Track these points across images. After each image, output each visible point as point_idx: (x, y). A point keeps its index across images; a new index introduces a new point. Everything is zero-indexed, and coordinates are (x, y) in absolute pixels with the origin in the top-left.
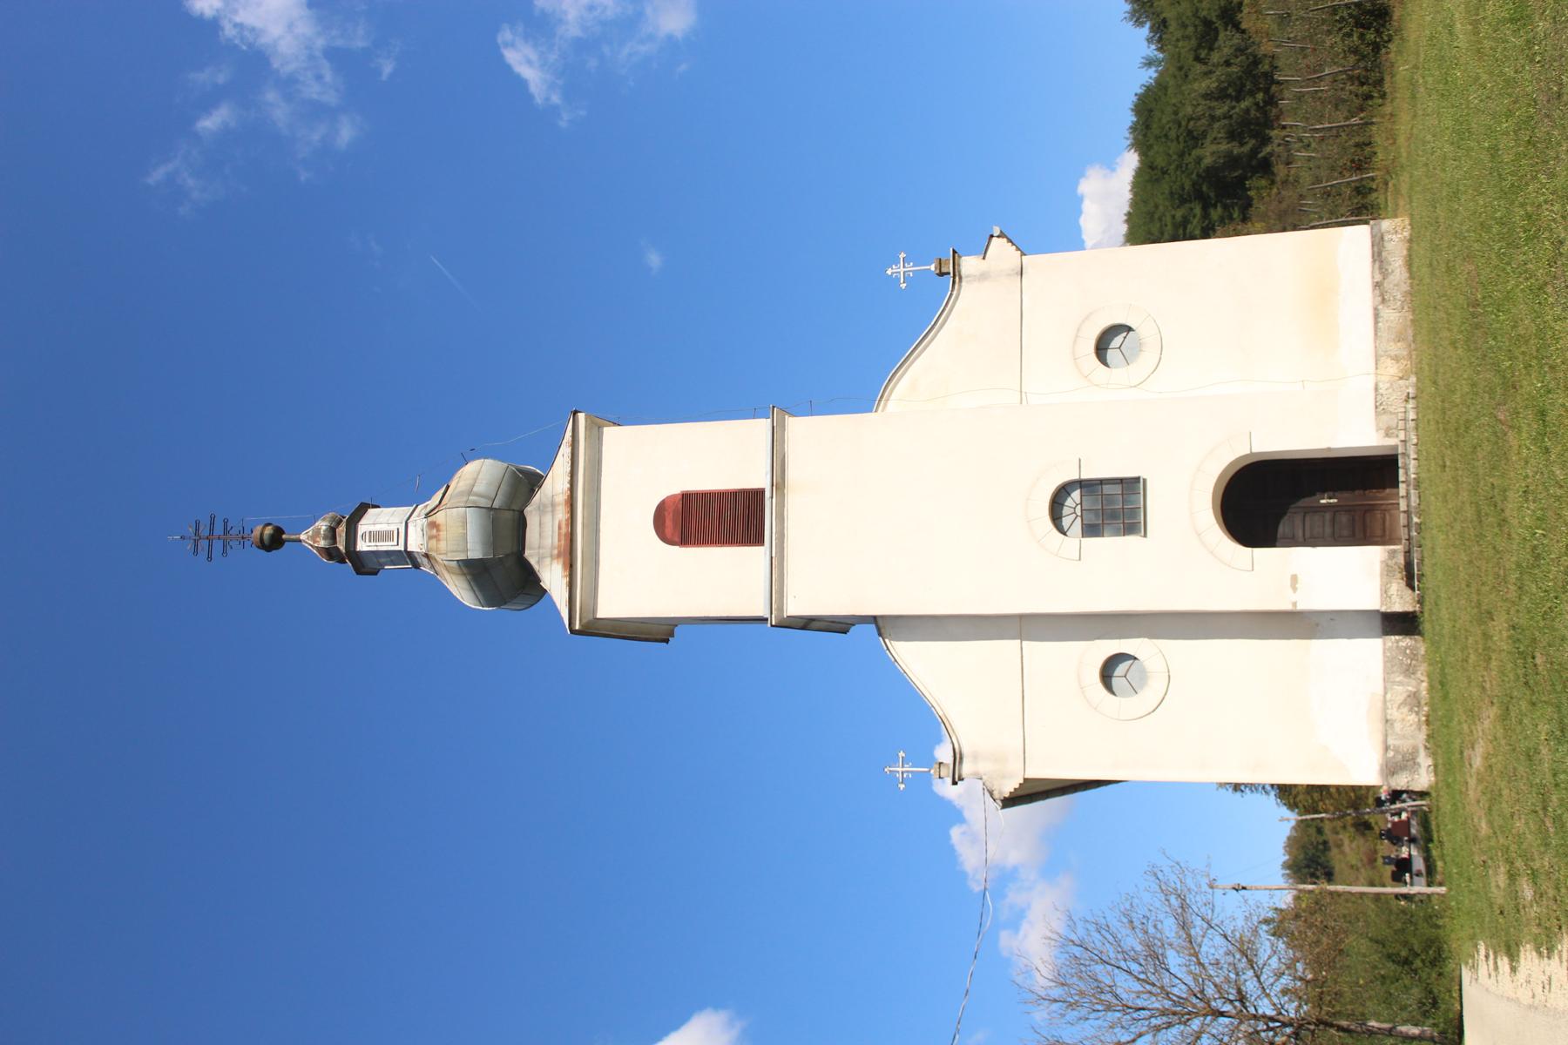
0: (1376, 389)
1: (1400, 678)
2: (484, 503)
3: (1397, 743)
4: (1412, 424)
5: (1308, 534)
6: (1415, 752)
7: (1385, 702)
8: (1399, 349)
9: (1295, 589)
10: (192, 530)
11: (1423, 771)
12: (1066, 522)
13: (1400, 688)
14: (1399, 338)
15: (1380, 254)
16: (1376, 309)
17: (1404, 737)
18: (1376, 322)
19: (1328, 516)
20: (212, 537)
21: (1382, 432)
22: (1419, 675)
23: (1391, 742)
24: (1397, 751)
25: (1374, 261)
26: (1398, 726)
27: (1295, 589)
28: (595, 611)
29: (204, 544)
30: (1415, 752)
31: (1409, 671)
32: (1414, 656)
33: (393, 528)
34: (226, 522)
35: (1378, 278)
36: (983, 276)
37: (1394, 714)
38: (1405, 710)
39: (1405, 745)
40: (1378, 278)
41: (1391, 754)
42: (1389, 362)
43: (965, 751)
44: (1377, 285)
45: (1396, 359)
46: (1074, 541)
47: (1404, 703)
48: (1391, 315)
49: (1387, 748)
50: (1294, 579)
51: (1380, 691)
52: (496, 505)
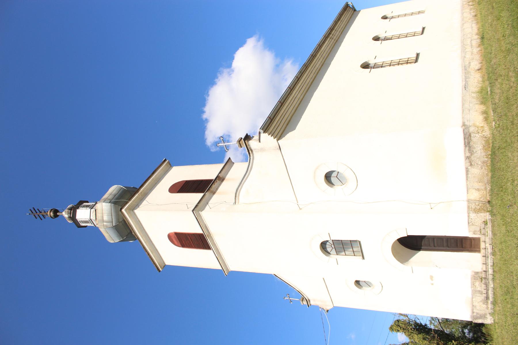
0: (469, 216)
2: (109, 224)
3: (478, 312)
4: (490, 277)
5: (436, 245)
7: (472, 301)
8: (480, 186)
9: (432, 280)
10: (30, 212)
12: (329, 250)
14: (480, 181)
15: (469, 143)
16: (467, 168)
18: (467, 174)
19: (444, 240)
20: (37, 213)
21: (472, 233)
23: (474, 311)
24: (477, 313)
25: (466, 146)
26: (478, 308)
27: (432, 280)
28: (164, 263)
29: (37, 216)
33: (88, 220)
34: (38, 209)
35: (468, 154)
36: (262, 150)
37: (475, 304)
38: (481, 303)
40: (468, 154)
41: (475, 314)
42: (474, 190)
43: (310, 298)
44: (468, 158)
45: (478, 190)
46: (334, 257)
47: (481, 301)
48: (476, 171)
50: (432, 277)
51: (470, 296)
52: (114, 225)
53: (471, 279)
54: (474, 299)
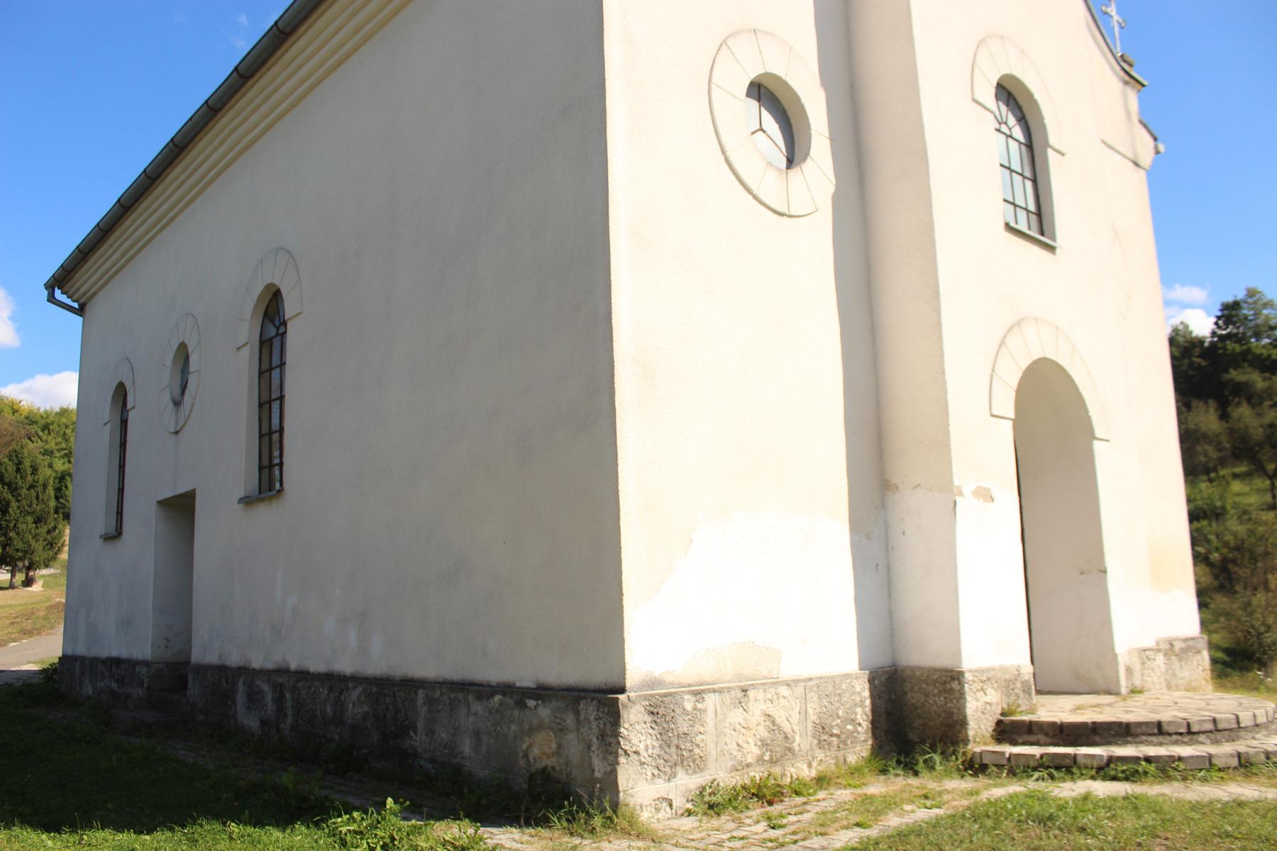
1: (813, 709)
3: (710, 718)
6: (695, 763)
11: (662, 787)
13: (795, 716)
17: (720, 734)
22: (820, 755)
23: (711, 701)
24: (696, 716)
26: (736, 716)
30: (695, 763)
31: (823, 732)
32: (844, 741)
37: (758, 705)
39: (707, 740)
40: (1178, 645)
49: (698, 694)
53: (1003, 669)
54: (784, 691)
